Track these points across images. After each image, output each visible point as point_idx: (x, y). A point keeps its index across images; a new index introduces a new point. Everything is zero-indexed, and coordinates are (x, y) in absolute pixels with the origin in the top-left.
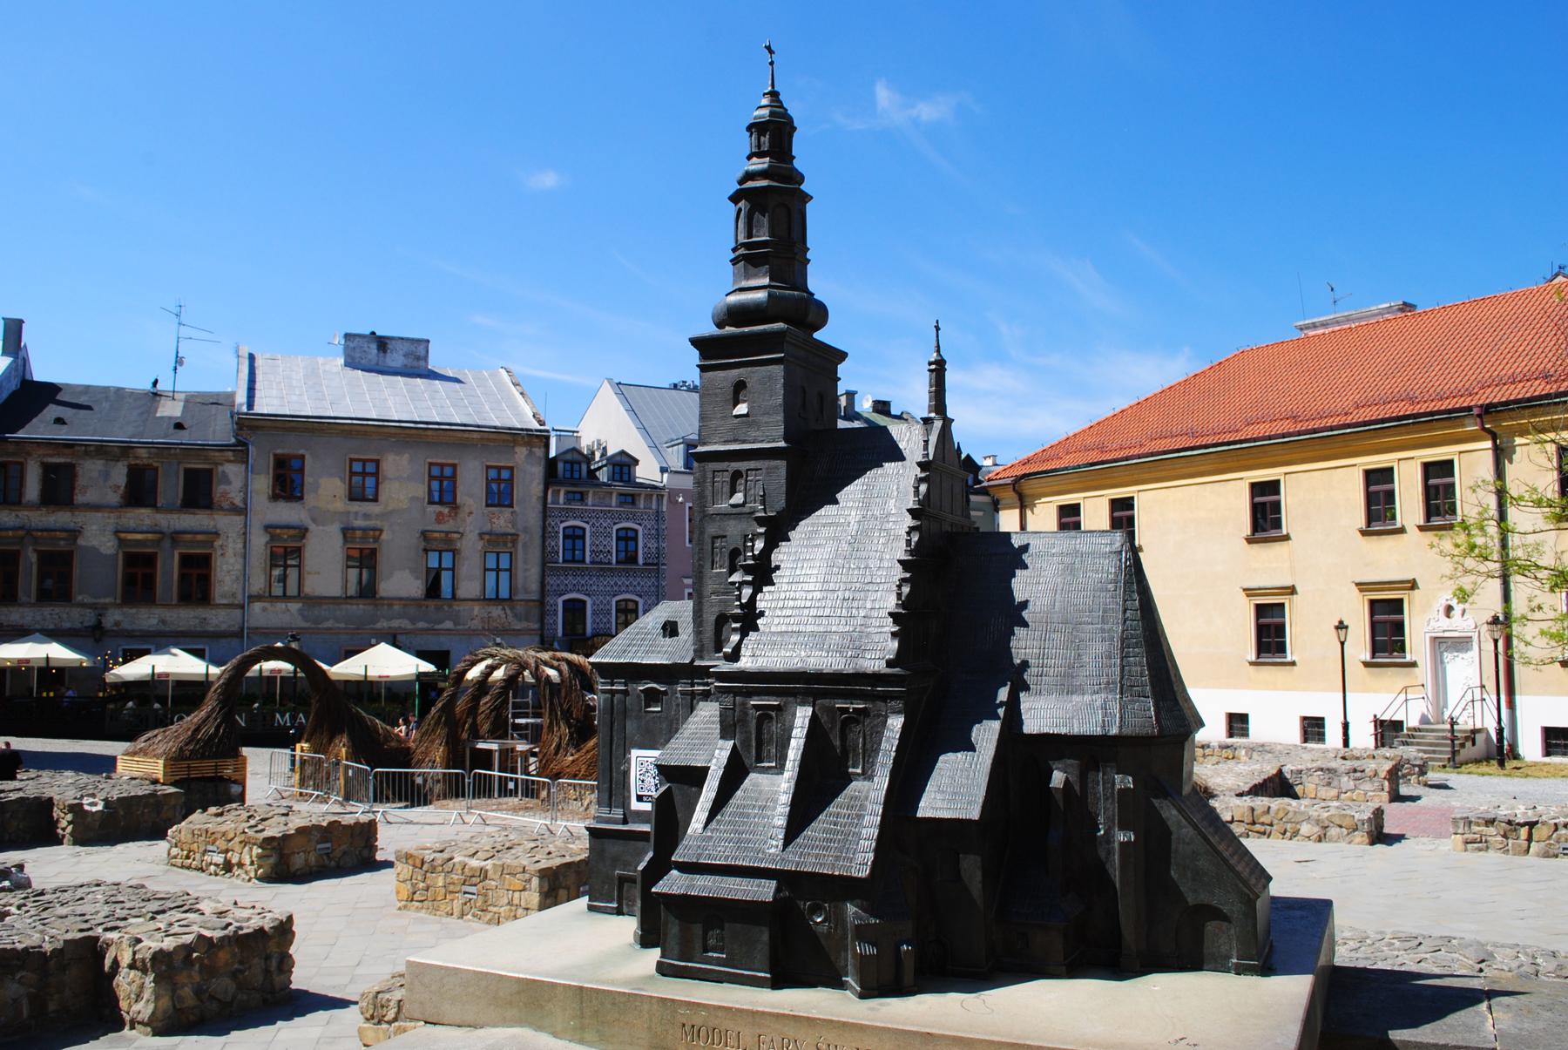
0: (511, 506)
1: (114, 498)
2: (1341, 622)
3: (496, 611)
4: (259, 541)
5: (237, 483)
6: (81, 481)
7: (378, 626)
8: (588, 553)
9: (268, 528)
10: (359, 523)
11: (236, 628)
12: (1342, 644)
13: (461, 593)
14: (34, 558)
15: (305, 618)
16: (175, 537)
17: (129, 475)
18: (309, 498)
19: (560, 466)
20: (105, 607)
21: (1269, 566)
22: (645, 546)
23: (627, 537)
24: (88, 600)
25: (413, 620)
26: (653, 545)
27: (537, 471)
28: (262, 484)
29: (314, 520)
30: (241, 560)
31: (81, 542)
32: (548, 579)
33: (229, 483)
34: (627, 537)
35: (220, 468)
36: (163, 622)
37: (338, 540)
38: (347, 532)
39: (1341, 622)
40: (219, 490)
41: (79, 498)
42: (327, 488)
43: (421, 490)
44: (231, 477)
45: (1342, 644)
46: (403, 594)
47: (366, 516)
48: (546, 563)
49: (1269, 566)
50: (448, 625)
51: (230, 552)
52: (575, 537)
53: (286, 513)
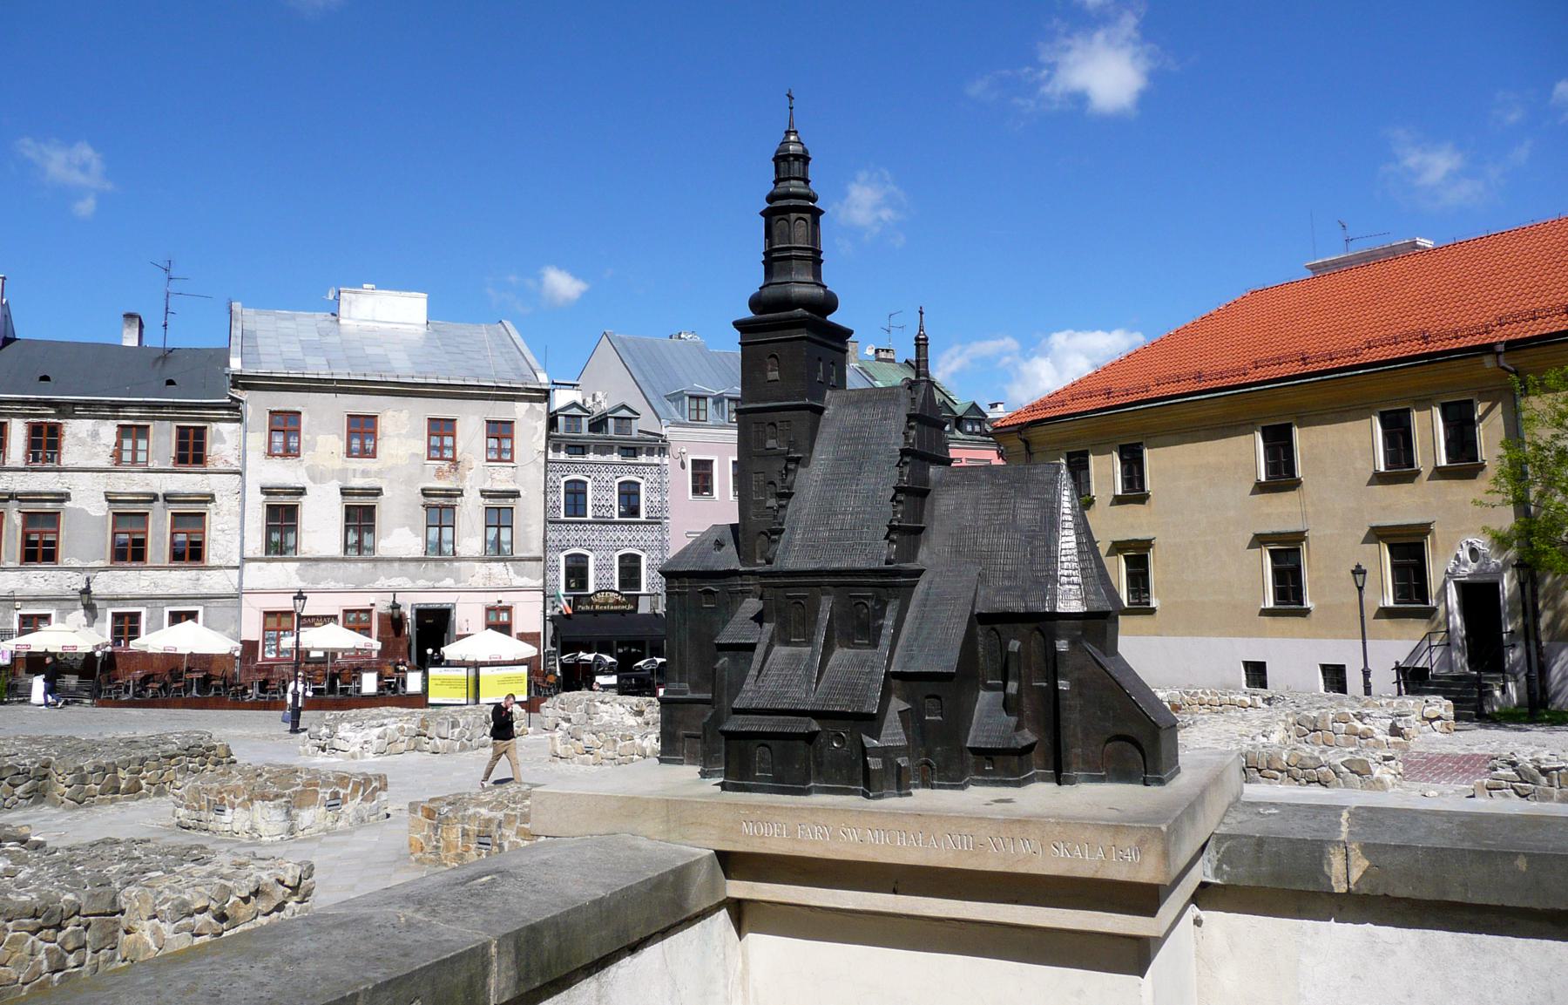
0: (512, 460)
1: (104, 461)
2: (1358, 566)
3: (497, 567)
6: (67, 443)
7: (378, 585)
8: (589, 508)
9: (266, 491)
10: (357, 482)
11: (231, 590)
12: (1360, 589)
13: (462, 551)
14: (17, 520)
15: (302, 578)
16: (169, 498)
19: (561, 420)
21: (1280, 513)
22: (648, 499)
23: (629, 494)
25: (413, 579)
26: (656, 498)
27: (542, 425)
28: (258, 440)
29: (313, 479)
30: (237, 521)
32: (549, 534)
33: (223, 441)
34: (629, 494)
36: (156, 586)
38: (345, 492)
39: (1358, 566)
40: (213, 449)
43: (420, 446)
45: (1360, 589)
47: (365, 473)
48: (550, 522)
49: (1280, 513)
50: (449, 582)
51: (225, 508)
52: (576, 493)
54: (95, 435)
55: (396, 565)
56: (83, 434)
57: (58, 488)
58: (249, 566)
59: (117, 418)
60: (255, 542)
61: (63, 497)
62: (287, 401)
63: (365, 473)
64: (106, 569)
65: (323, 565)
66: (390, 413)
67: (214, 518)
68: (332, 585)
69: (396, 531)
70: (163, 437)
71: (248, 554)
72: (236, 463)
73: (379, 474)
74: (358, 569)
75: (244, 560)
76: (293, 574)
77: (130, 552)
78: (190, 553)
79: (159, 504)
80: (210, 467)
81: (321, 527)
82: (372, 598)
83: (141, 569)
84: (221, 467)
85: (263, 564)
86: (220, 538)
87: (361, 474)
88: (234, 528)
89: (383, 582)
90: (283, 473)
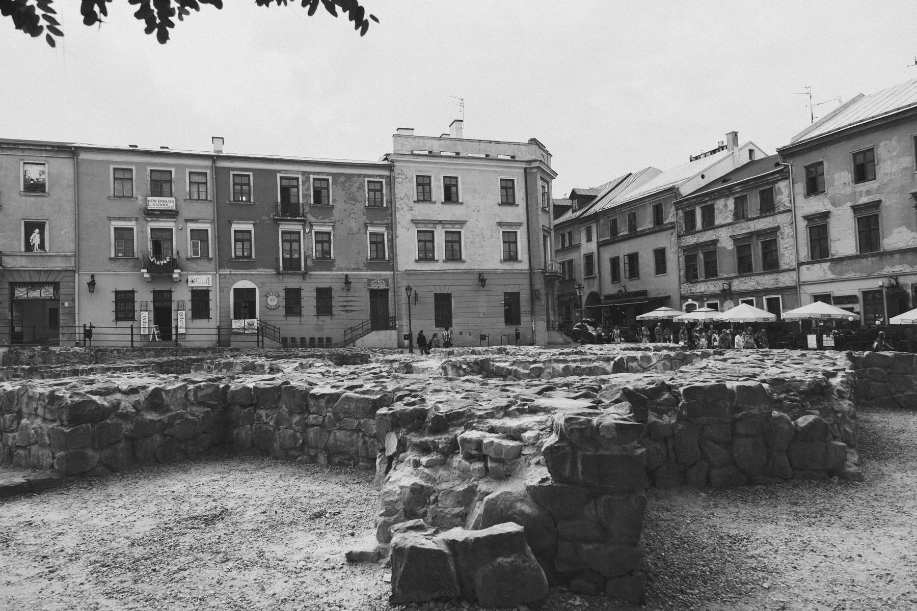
4: (802, 224)
5: (785, 192)
7: (885, 272)
10: (864, 200)
11: (793, 284)
14: (701, 256)
15: (833, 272)
17: (735, 203)
18: (830, 191)
20: (731, 278)
24: (725, 276)
28: (801, 188)
31: (719, 245)
35: (777, 186)
36: (758, 284)
37: (850, 214)
41: (717, 222)
42: (839, 178)
44: (783, 189)
46: (902, 245)
53: (816, 205)
54: (726, 206)
55: (897, 256)
56: (721, 207)
57: (714, 238)
58: (804, 268)
59: (733, 194)
60: (804, 253)
61: (715, 242)
62: (813, 158)
63: (868, 193)
64: (736, 277)
65: (845, 263)
66: (882, 144)
67: (781, 241)
68: (852, 275)
69: (896, 230)
70: (754, 202)
71: (802, 260)
72: (789, 205)
73: (879, 190)
74: (868, 262)
75: (800, 264)
76: (827, 271)
77: (745, 268)
78: (771, 264)
79: (754, 239)
80: (777, 211)
81: (844, 239)
82: (880, 283)
83: (750, 276)
84: (782, 209)
85: (809, 266)
86: (787, 253)
87: (865, 193)
88: (792, 247)
89: (888, 270)
90: (816, 205)
